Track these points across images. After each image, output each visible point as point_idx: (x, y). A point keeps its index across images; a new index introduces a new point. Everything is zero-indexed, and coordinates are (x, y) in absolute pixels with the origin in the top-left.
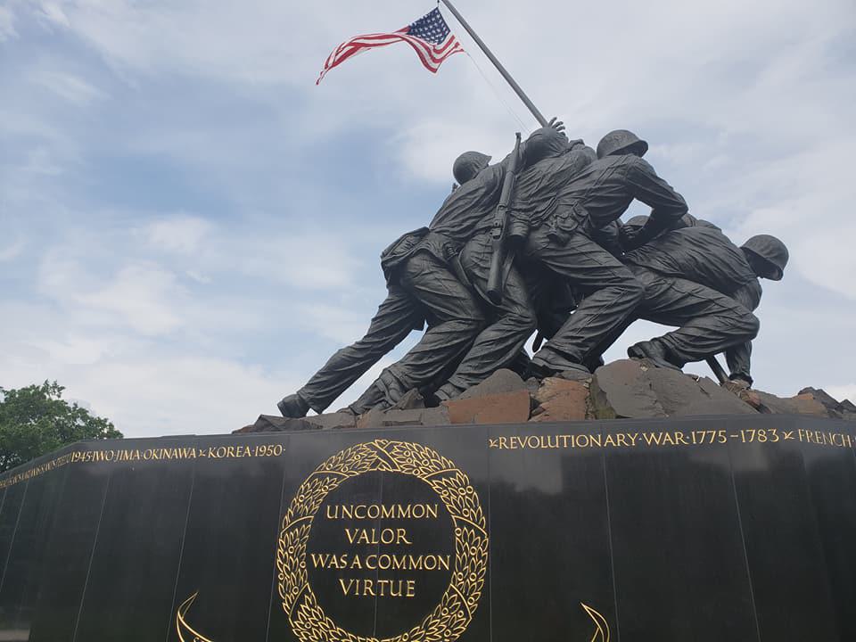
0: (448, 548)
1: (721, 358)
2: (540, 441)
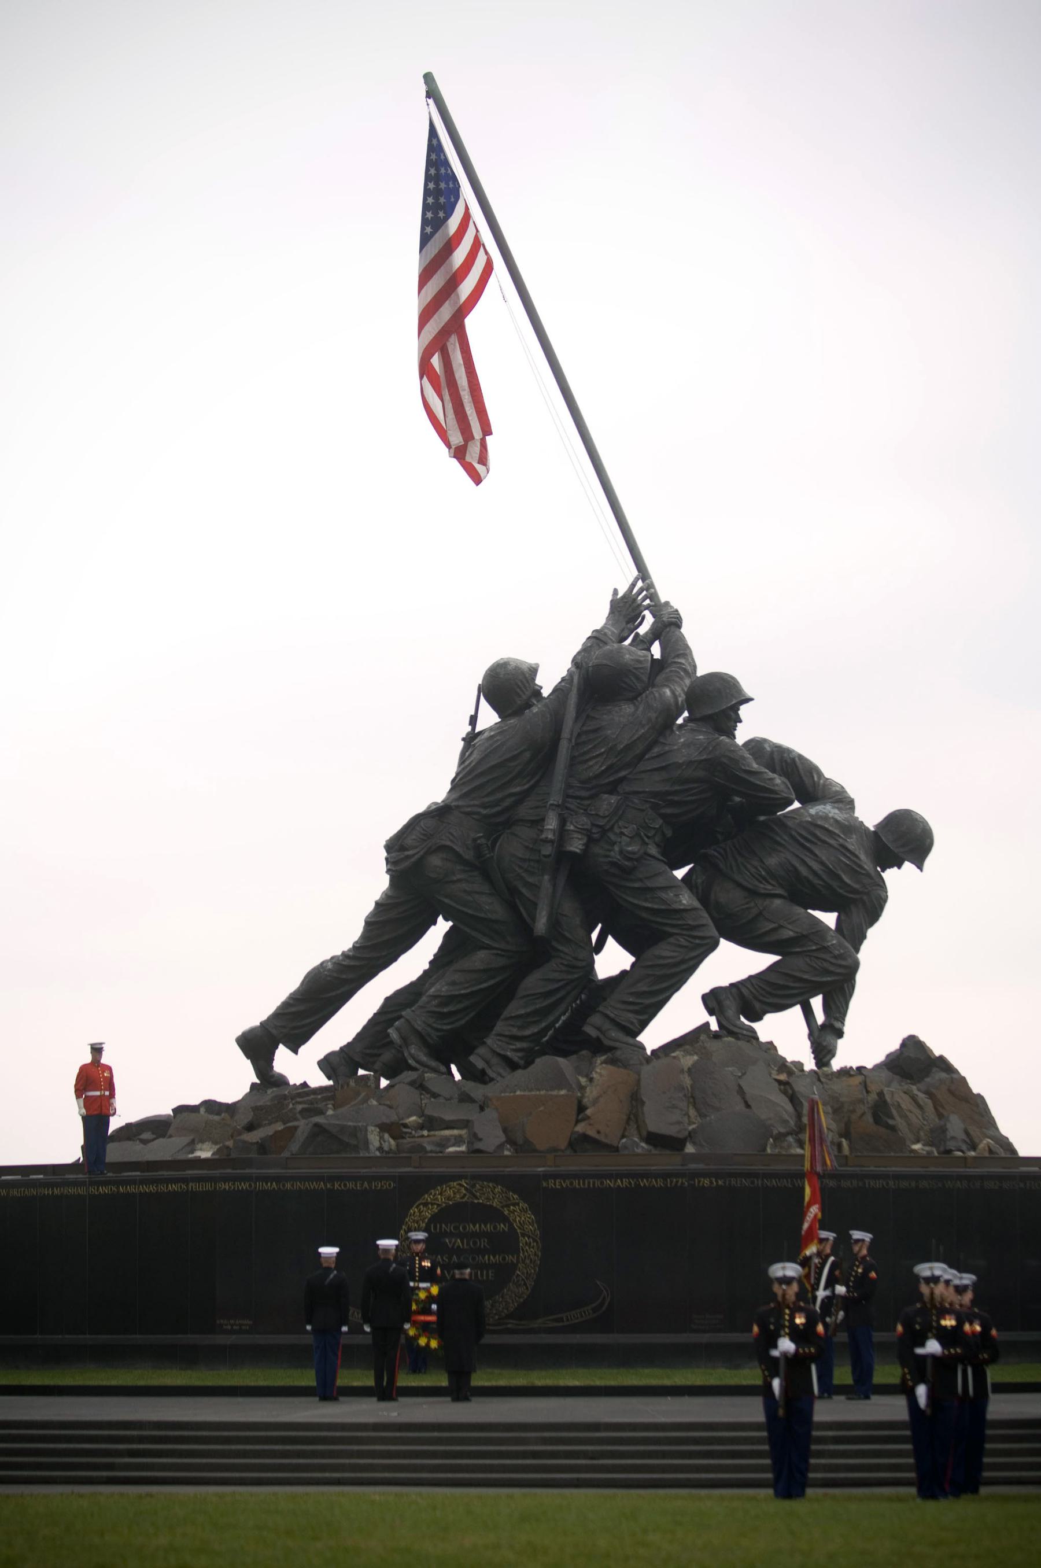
2: (576, 1183)
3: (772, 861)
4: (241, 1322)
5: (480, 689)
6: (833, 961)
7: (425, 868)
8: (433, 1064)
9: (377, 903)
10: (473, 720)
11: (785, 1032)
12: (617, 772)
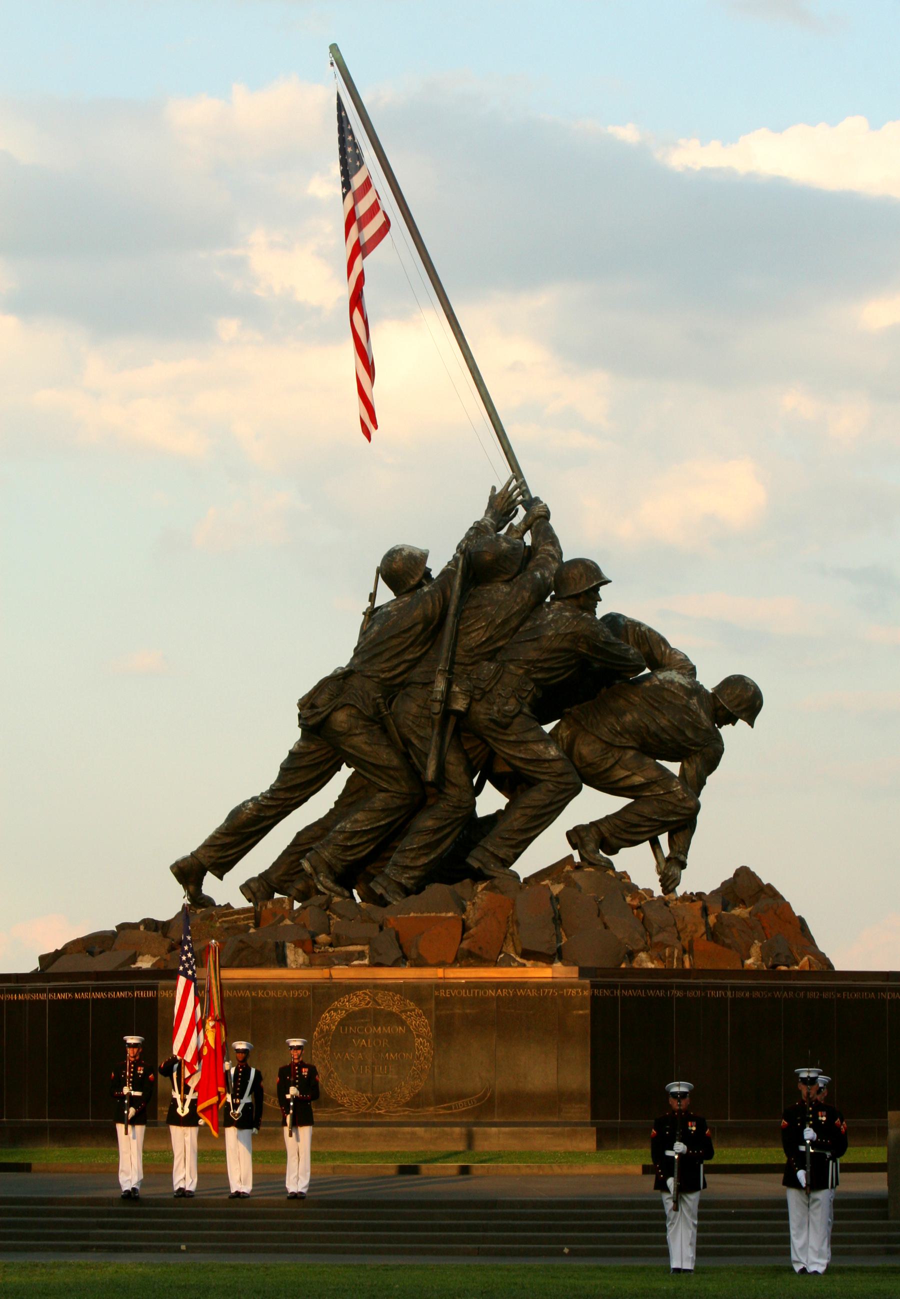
1: (664, 839)
5: (379, 571)
6: (677, 803)
7: (329, 723)
8: (338, 889)
9: (291, 753)
10: (372, 597)
11: (637, 864)
12: (495, 642)
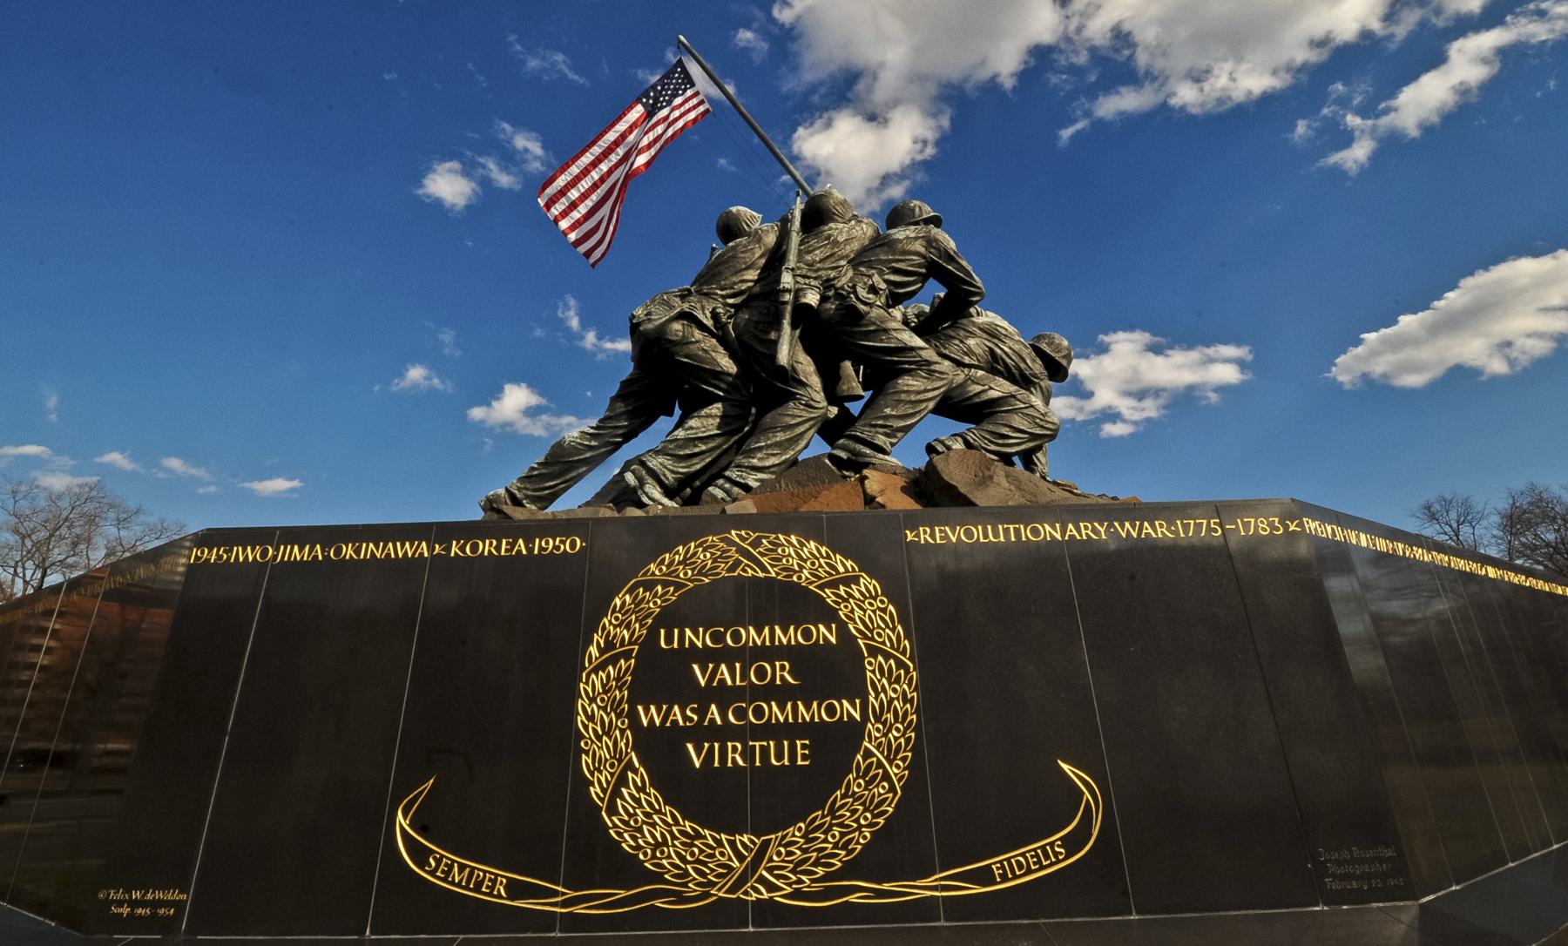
0: (856, 690)
2: (977, 532)
3: (971, 342)
4: (159, 895)
